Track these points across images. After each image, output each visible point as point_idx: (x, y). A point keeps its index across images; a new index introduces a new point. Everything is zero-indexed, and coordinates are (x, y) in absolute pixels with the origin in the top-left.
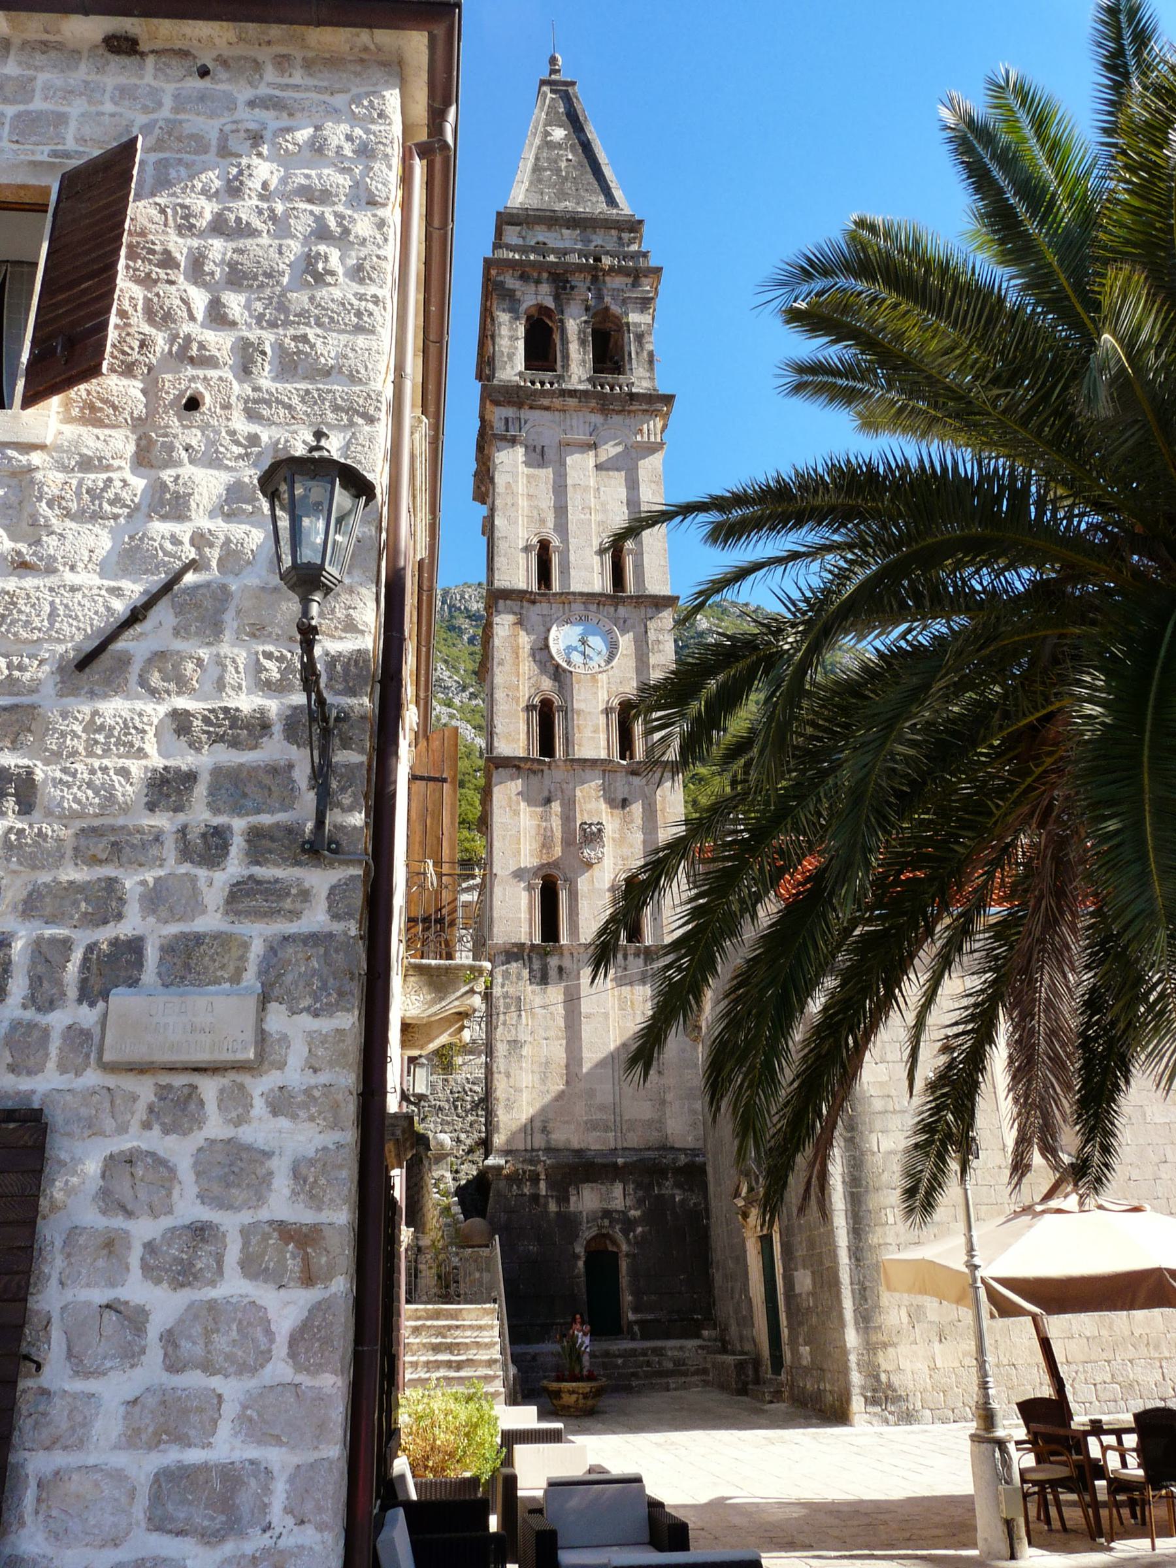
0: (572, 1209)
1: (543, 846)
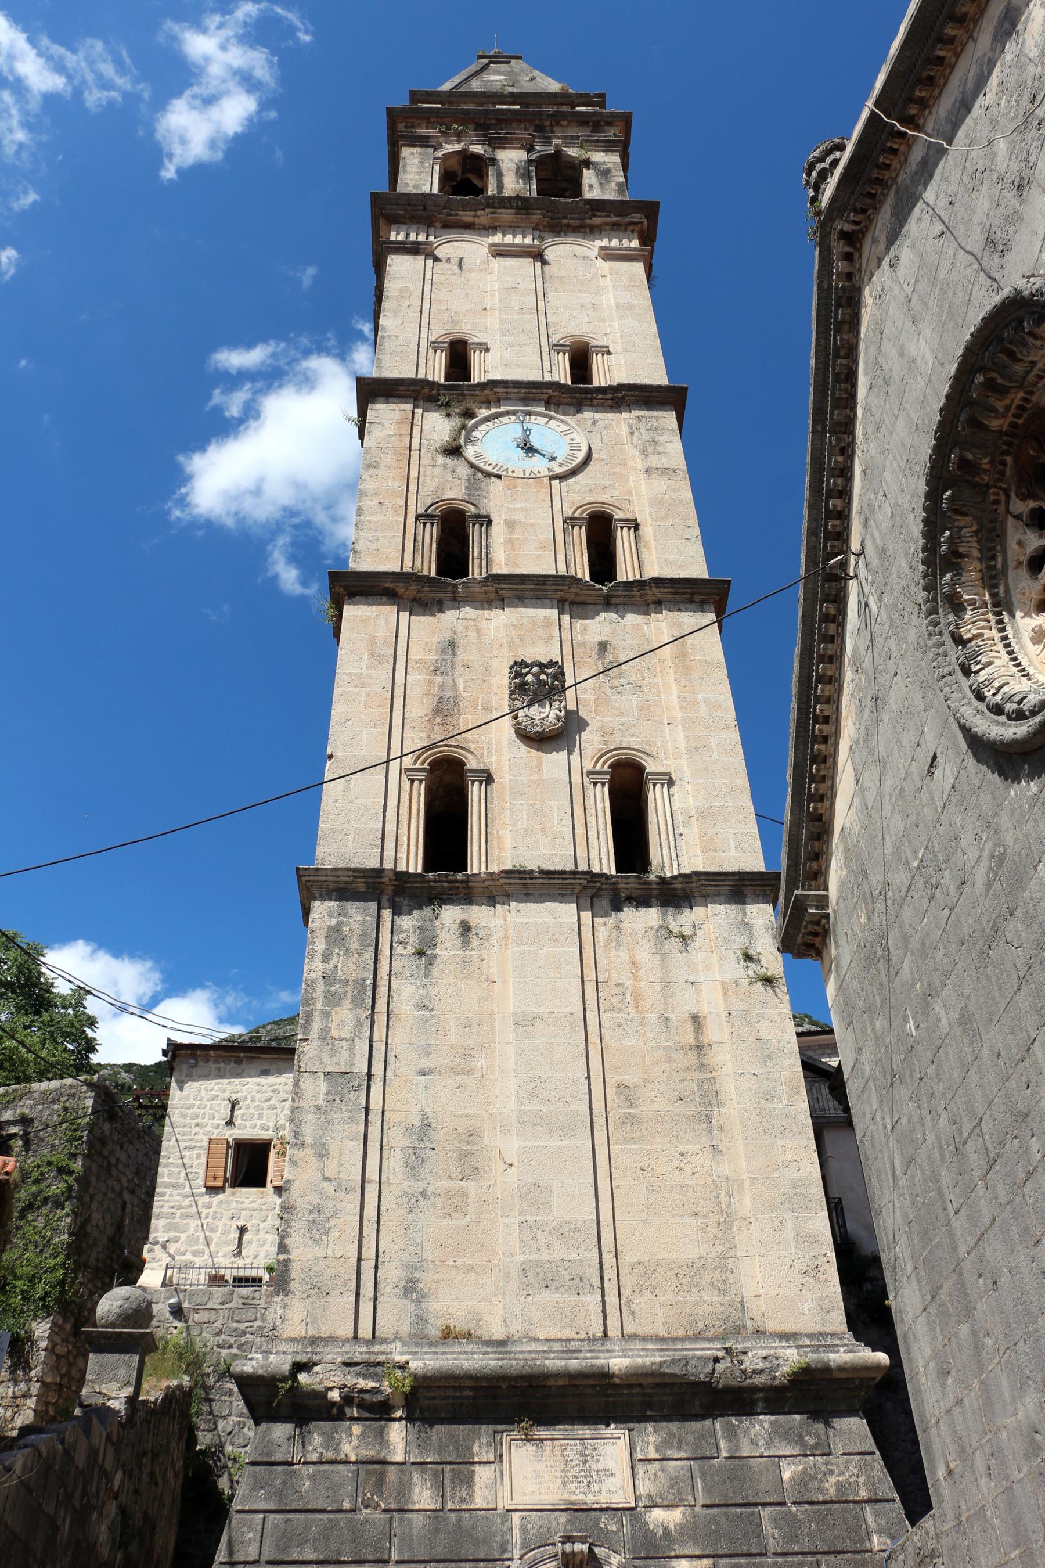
0: (479, 1502)
1: (437, 711)
